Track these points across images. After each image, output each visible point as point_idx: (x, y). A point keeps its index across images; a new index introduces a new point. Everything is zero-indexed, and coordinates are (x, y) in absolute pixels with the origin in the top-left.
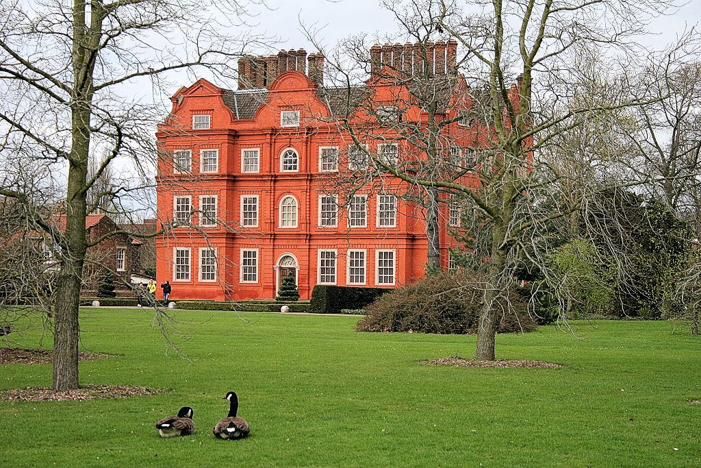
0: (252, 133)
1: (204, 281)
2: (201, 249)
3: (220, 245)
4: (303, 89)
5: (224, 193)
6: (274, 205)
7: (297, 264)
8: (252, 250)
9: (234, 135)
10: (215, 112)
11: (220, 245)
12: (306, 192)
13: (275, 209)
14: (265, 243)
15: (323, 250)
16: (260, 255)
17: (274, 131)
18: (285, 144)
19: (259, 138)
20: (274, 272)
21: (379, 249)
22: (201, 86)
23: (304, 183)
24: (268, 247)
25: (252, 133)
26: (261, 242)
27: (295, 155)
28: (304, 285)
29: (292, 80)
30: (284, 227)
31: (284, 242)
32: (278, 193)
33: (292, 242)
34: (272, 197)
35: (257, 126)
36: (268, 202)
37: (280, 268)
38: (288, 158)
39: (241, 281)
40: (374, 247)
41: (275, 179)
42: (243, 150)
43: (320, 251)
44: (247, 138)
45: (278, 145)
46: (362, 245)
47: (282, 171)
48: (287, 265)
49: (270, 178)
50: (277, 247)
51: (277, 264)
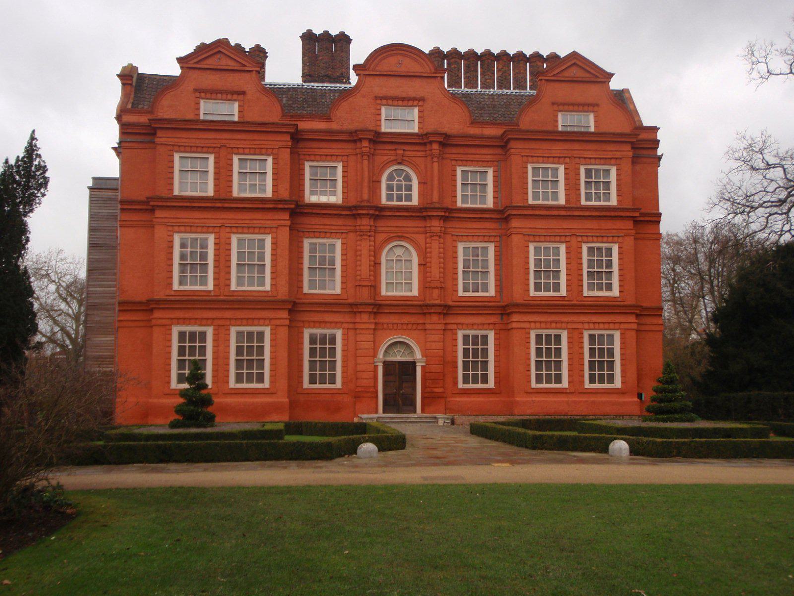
0: (330, 137)
1: (239, 386)
2: (233, 330)
3: (278, 322)
4: (424, 75)
5: (285, 234)
6: (374, 256)
7: (418, 355)
8: (328, 332)
9: (297, 137)
10: (248, 97)
11: (278, 322)
12: (439, 237)
13: (376, 265)
14: (358, 320)
15: (467, 332)
16: (345, 339)
17: (378, 139)
18: (393, 158)
19: (340, 145)
20: (376, 367)
21: (589, 329)
22: (220, 52)
23: (435, 223)
24: (366, 326)
25: (330, 137)
26: (348, 318)
27: (408, 178)
28: (436, 390)
29: (401, 58)
30: (389, 294)
31: (394, 319)
32: (381, 237)
33: (413, 319)
34: (372, 243)
35: (335, 126)
36: (365, 252)
37: (386, 364)
38: (395, 183)
39: (306, 385)
40: (580, 326)
41: (379, 213)
42: (307, 165)
43: (460, 334)
44: (314, 145)
45: (379, 160)
46: (560, 325)
47: (384, 201)
48: (399, 356)
49: (371, 212)
50: (380, 327)
51: (380, 355)
